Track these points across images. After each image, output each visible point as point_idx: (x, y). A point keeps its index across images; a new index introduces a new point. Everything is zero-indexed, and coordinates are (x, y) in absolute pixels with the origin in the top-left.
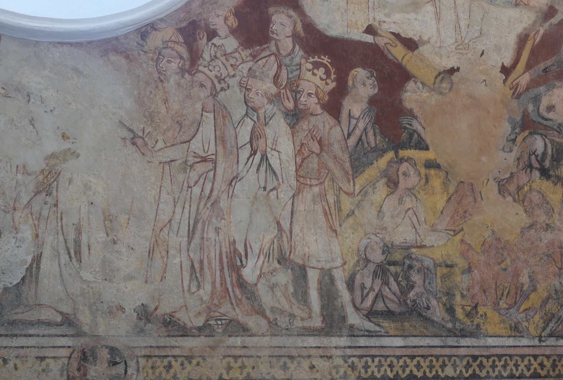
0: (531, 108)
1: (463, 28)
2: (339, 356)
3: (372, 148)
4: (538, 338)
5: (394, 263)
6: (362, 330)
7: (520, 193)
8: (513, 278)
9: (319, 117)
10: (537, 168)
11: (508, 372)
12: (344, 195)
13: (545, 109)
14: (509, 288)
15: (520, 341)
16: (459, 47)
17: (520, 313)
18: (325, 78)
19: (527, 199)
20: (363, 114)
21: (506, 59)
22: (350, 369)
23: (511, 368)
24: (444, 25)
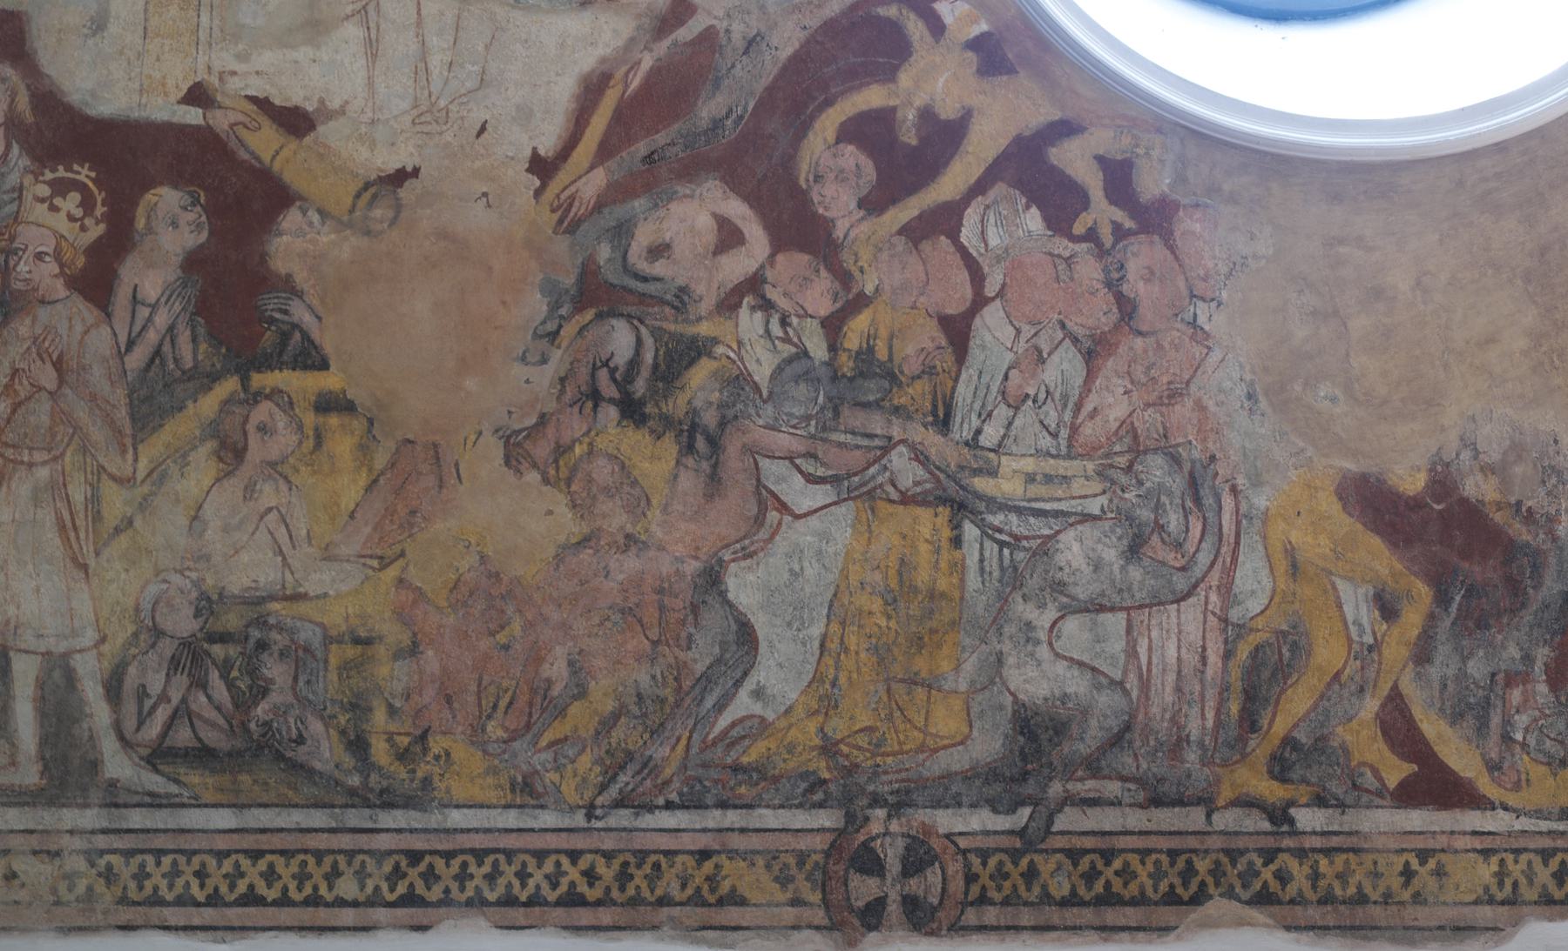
0: (604, 252)
1: (435, 73)
2: (78, 852)
3: (184, 373)
4: (584, 811)
5: (223, 638)
6: (137, 793)
7: (561, 463)
8: (525, 666)
9: (59, 306)
10: (611, 401)
11: (500, 890)
12: (111, 483)
13: (644, 254)
14: (515, 692)
15: (535, 818)
16: (423, 119)
17: (540, 751)
18: (81, 214)
19: (579, 475)
20: (168, 292)
21: (543, 138)
22: (102, 881)
23: (510, 882)
24: (388, 68)
